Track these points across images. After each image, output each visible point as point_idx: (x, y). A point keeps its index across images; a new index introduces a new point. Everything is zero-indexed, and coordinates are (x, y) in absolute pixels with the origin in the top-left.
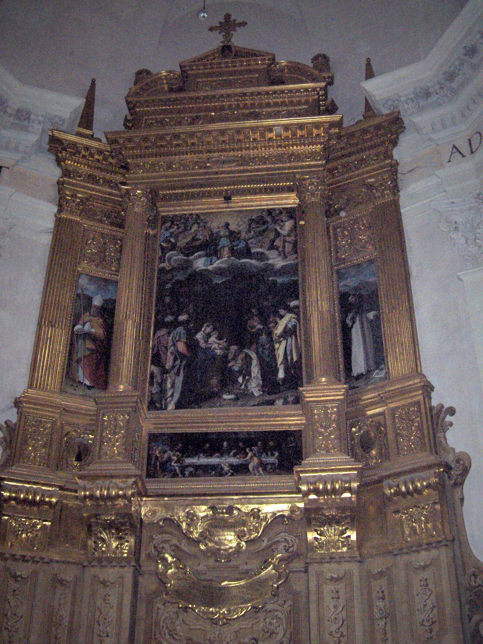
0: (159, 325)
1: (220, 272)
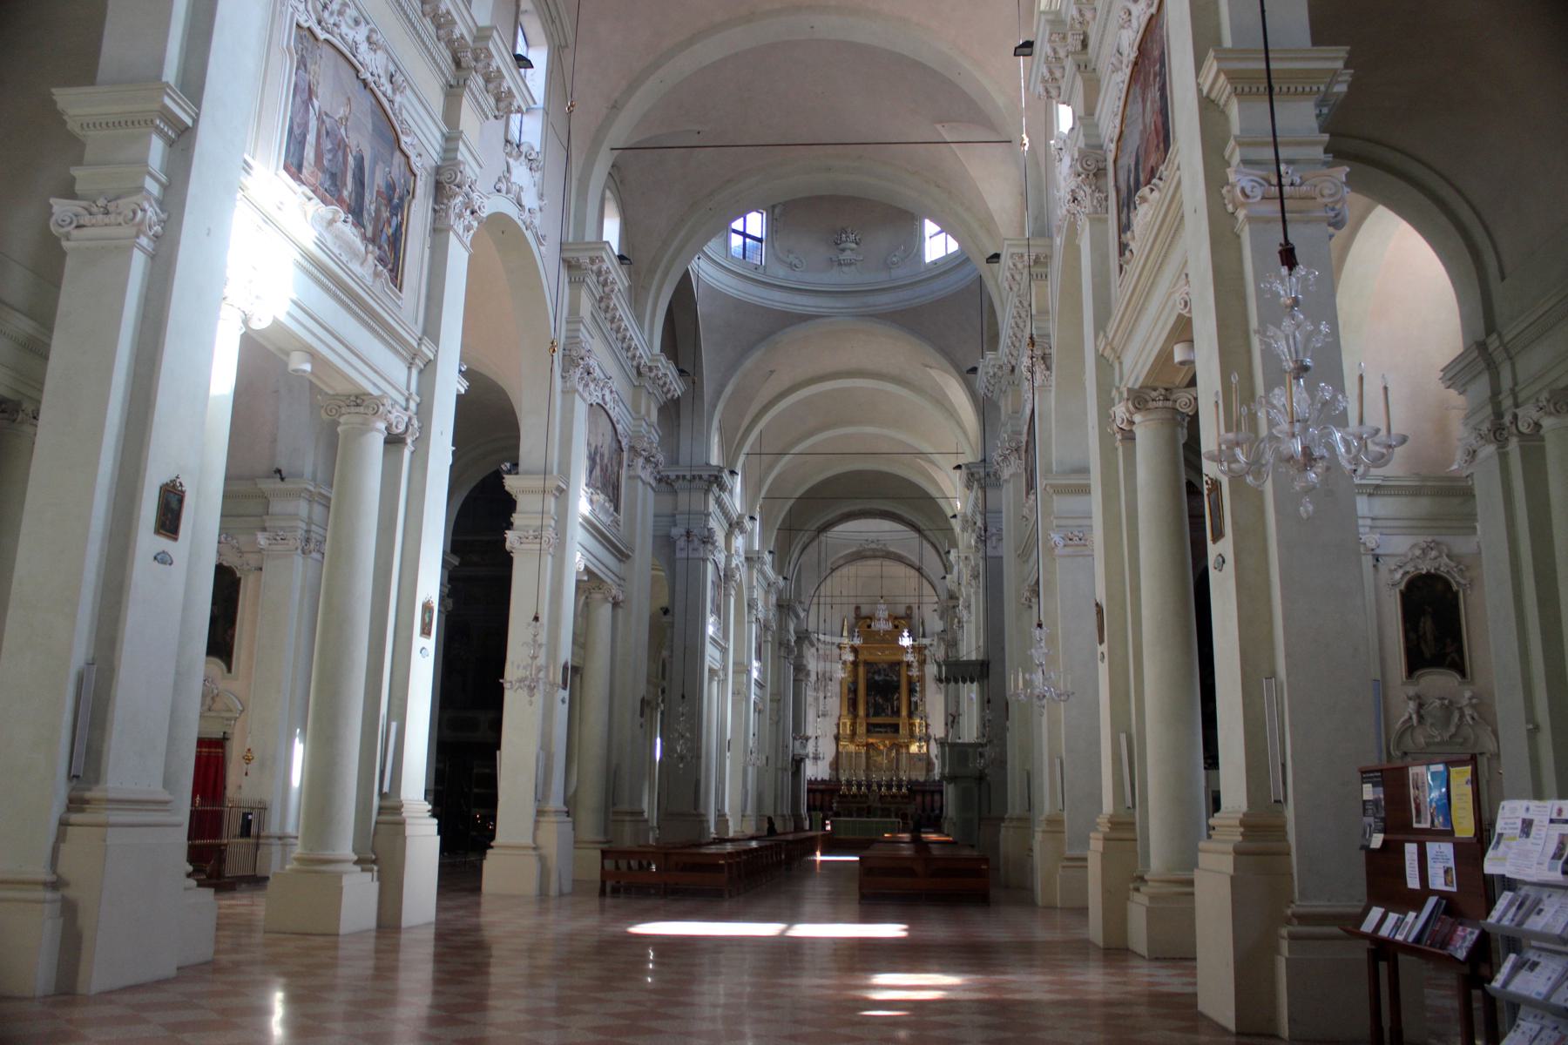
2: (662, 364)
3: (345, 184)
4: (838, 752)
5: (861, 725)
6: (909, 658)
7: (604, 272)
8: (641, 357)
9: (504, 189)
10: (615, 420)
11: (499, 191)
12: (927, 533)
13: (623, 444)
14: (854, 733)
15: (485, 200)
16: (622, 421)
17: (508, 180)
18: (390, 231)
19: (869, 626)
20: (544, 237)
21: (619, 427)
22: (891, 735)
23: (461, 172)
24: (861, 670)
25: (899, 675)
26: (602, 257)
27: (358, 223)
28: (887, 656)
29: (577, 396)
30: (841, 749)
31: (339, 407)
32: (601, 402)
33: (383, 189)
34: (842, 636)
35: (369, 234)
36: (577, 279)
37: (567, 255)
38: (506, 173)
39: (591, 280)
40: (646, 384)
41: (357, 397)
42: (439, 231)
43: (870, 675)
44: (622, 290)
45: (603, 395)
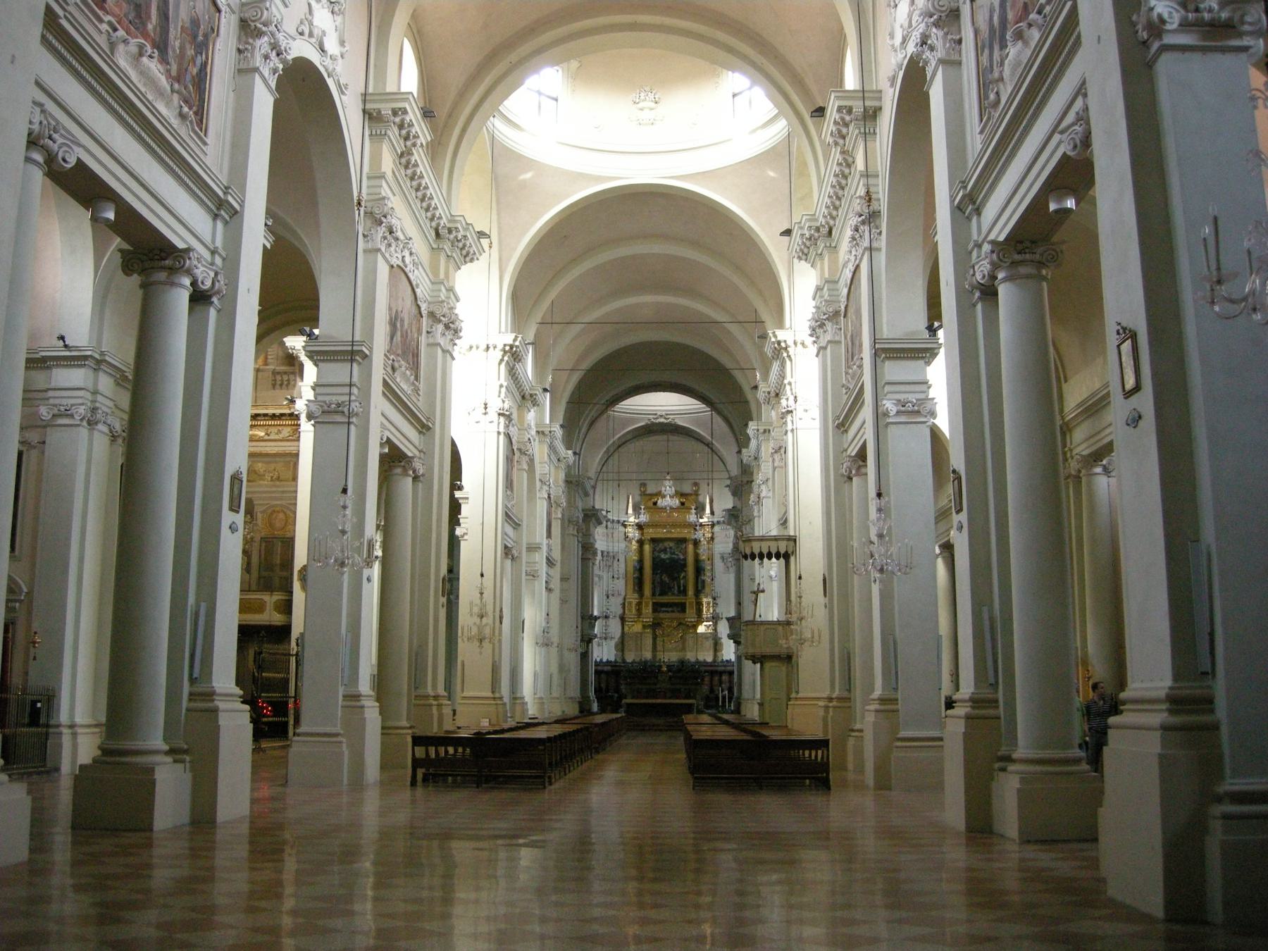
0: (653, 574)
1: (668, 559)
2: (463, 227)
3: (149, 17)
4: (623, 633)
5: (647, 605)
6: (699, 535)
7: (406, 125)
8: (440, 218)
9: (307, 32)
10: (414, 283)
11: (302, 34)
12: (720, 406)
13: (422, 309)
14: (639, 611)
15: (291, 41)
16: (421, 285)
17: (311, 24)
18: (195, 71)
19: (655, 504)
20: (346, 86)
21: (418, 291)
22: (676, 615)
23: (267, 9)
24: (647, 548)
25: (685, 553)
26: (405, 109)
27: (164, 60)
28: (677, 533)
29: (379, 256)
30: (626, 628)
31: (142, 262)
32: (402, 265)
33: (187, 25)
34: (627, 513)
35: (174, 73)
36: (378, 133)
37: (368, 106)
38: (308, 16)
39: (393, 132)
40: (445, 247)
41: (161, 250)
42: (245, 71)
43: (657, 554)
44: (424, 144)
45: (403, 257)
